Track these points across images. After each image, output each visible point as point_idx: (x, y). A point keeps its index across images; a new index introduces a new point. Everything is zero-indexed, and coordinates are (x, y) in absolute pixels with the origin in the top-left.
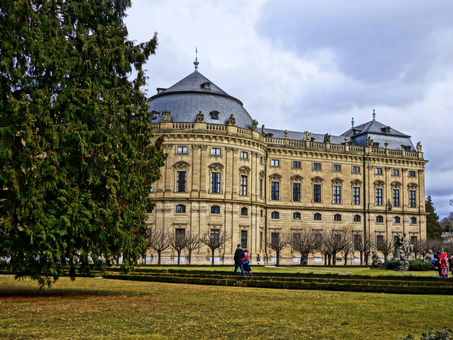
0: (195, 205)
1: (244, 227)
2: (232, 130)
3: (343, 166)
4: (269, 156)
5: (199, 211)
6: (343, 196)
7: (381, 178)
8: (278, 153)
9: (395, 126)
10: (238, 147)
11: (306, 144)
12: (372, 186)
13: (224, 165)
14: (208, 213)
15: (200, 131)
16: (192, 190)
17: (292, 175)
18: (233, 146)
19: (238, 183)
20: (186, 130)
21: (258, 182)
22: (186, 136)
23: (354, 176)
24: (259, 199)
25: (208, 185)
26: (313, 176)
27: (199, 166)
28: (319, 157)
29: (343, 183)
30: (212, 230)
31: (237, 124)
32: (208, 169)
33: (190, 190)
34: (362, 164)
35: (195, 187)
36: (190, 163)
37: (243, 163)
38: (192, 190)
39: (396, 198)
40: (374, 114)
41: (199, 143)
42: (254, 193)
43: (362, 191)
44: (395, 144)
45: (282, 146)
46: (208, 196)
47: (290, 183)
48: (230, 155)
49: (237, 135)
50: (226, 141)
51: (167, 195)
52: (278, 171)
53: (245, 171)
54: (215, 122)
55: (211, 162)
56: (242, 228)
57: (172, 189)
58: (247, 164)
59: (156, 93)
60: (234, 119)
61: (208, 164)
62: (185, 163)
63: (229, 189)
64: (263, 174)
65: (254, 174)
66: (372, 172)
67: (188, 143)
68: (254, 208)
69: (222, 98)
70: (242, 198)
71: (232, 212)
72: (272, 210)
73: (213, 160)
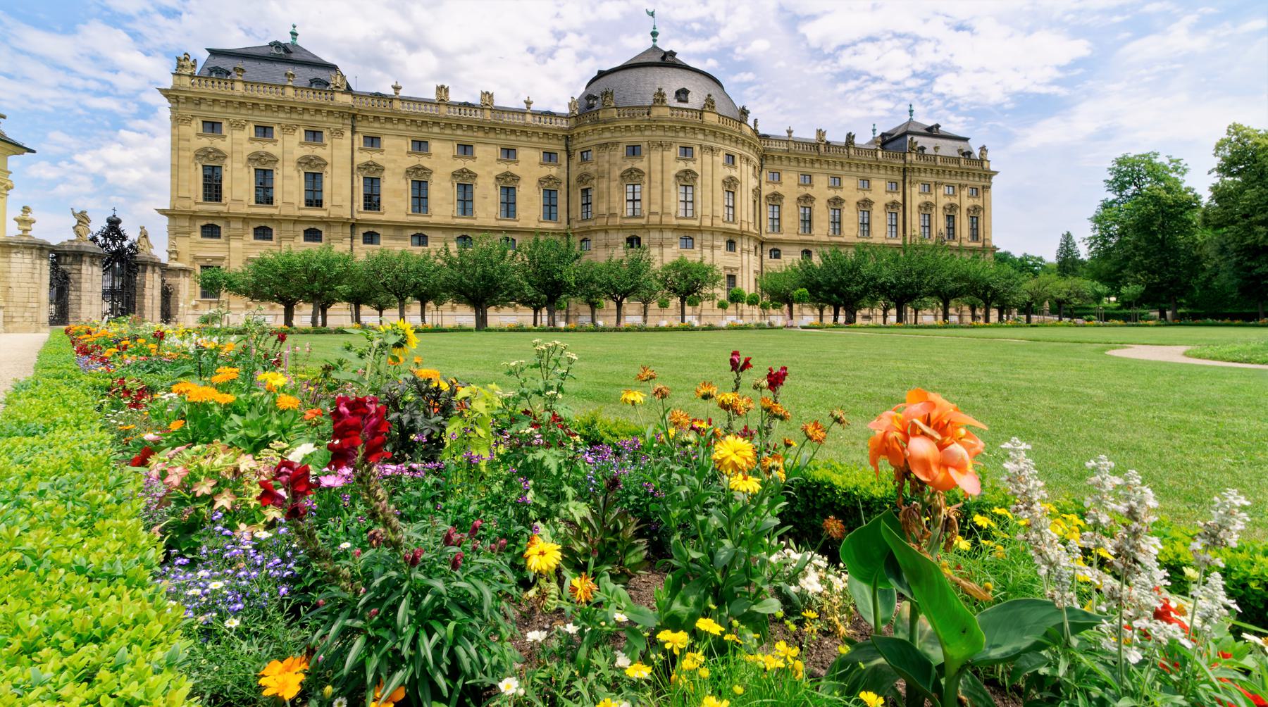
0: (655, 235)
1: (730, 269)
2: (710, 118)
3: (873, 183)
5: (661, 245)
6: (874, 225)
7: (930, 199)
8: (777, 162)
9: (945, 128)
11: (818, 153)
12: (915, 209)
14: (676, 248)
15: (659, 119)
16: (650, 213)
19: (720, 202)
21: (751, 203)
22: (638, 128)
23: (889, 195)
24: (751, 228)
27: (659, 176)
28: (839, 167)
29: (874, 207)
31: (717, 109)
33: (646, 213)
35: (655, 208)
36: (646, 171)
38: (650, 213)
39: (951, 228)
40: (911, 111)
41: (658, 139)
42: (744, 218)
43: (900, 217)
44: (948, 149)
48: (707, 158)
49: (717, 127)
50: (700, 136)
51: (611, 222)
52: (778, 189)
53: (731, 185)
56: (729, 272)
57: (618, 211)
60: (713, 102)
61: (674, 172)
62: (637, 170)
63: (708, 211)
64: (757, 192)
65: (744, 189)
66: (916, 189)
68: (745, 240)
70: (728, 226)
71: (713, 247)
73: (682, 166)
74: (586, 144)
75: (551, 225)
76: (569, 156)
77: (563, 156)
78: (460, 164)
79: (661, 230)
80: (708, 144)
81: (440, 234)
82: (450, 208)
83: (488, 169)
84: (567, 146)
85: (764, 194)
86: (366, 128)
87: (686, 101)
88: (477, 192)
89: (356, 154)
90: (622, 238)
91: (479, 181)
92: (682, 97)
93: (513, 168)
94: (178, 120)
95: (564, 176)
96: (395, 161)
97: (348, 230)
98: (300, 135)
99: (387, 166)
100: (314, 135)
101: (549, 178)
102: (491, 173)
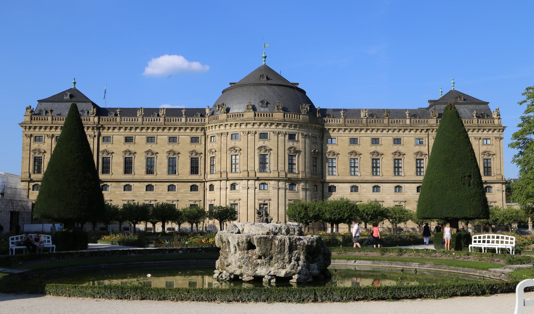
3: (404, 140)
4: (325, 135)
15: (248, 119)
17: (349, 151)
18: (280, 130)
20: (238, 119)
26: (372, 151)
32: (257, 151)
34: (427, 136)
38: (244, 171)
41: (247, 130)
45: (338, 125)
54: (262, 109)
55: (259, 146)
59: (230, 86)
61: (256, 147)
69: (275, 87)
74: (212, 133)
76: (205, 139)
77: (203, 138)
79: (248, 180)
82: (144, 170)
83: (162, 149)
86: (104, 133)
89: (101, 146)
90: (229, 183)
93: (175, 147)
96: (117, 148)
102: (163, 151)
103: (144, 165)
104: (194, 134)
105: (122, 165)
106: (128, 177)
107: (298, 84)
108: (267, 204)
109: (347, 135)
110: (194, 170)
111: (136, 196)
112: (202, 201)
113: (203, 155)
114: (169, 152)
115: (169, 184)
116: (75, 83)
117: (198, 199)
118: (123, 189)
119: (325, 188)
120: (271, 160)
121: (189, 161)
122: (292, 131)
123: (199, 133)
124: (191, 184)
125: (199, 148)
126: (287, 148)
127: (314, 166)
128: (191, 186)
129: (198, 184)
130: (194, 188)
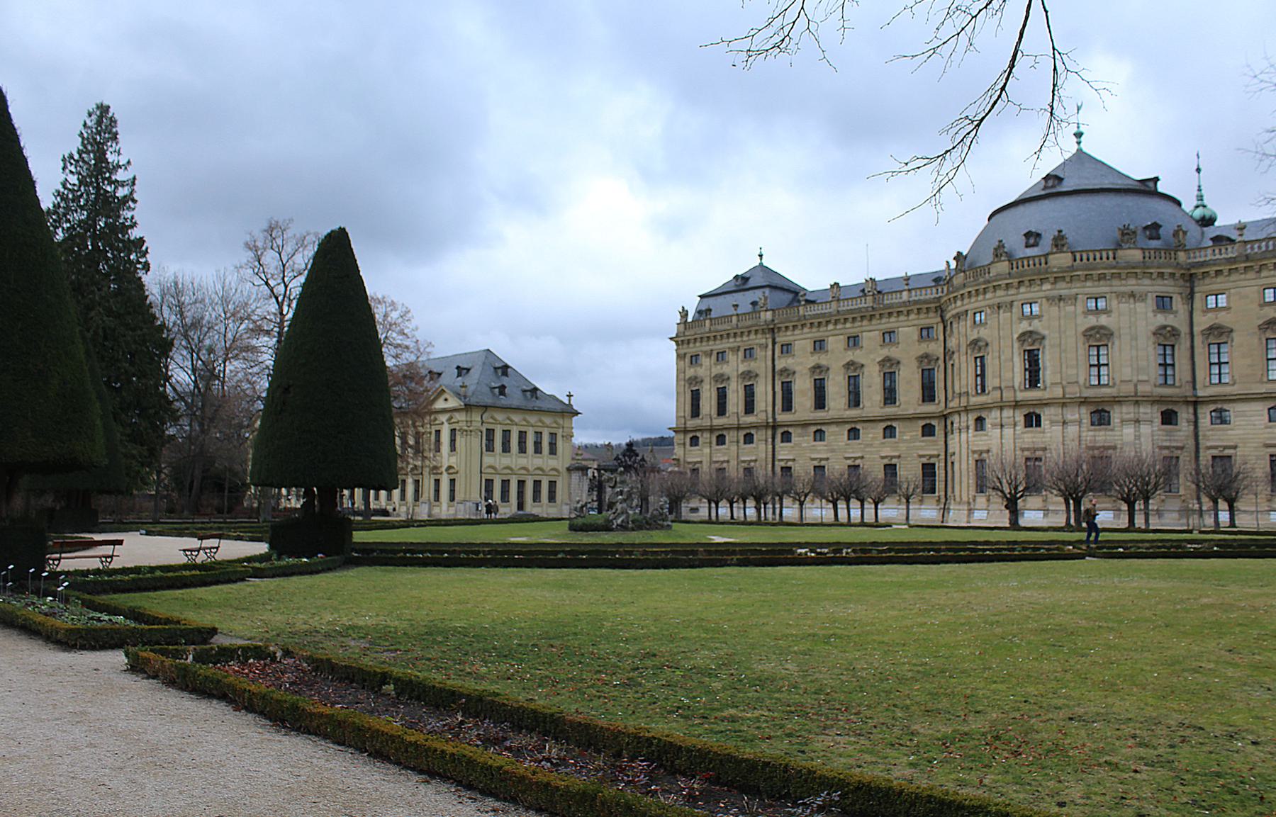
0: (995, 414)
4: (1196, 289)
8: (1220, 279)
10: (1074, 291)
13: (1046, 332)
14: (1020, 427)
15: (999, 277)
17: (1261, 322)
18: (1063, 292)
25: (1018, 374)
30: (1027, 459)
32: (1016, 345)
36: (989, 340)
37: (1092, 321)
38: (994, 388)
41: (998, 300)
46: (1021, 396)
47: (1256, 341)
49: (1072, 268)
52: (1224, 319)
55: (1021, 331)
58: (1103, 320)
60: (1063, 238)
61: (1016, 336)
67: (983, 303)
72: (1213, 407)
75: (929, 408)
76: (945, 328)
77: (941, 327)
78: (851, 356)
80: (1056, 293)
81: (833, 428)
84: (942, 317)
85: (1196, 329)
86: (781, 339)
87: (1035, 245)
88: (864, 382)
89: (776, 362)
91: (865, 369)
92: (1032, 241)
94: (680, 357)
95: (942, 350)
96: (801, 363)
97: (770, 432)
98: (741, 354)
99: (797, 369)
100: (749, 353)
101: (926, 356)
103: (845, 392)
104: (925, 320)
105: (811, 394)
106: (820, 415)
107: (1156, 180)
108: (1040, 460)
109: (1253, 282)
110: (928, 394)
111: (833, 451)
112: (942, 457)
113: (941, 362)
114: (882, 363)
115: (884, 425)
116: (761, 256)
117: (935, 453)
118: (812, 438)
119: (1200, 416)
120: (1047, 361)
121: (918, 376)
122: (1091, 288)
123: (933, 319)
124: (922, 423)
125: (936, 349)
126: (1082, 329)
127: (1164, 365)
128: (923, 427)
129: (934, 422)
130: (928, 431)
